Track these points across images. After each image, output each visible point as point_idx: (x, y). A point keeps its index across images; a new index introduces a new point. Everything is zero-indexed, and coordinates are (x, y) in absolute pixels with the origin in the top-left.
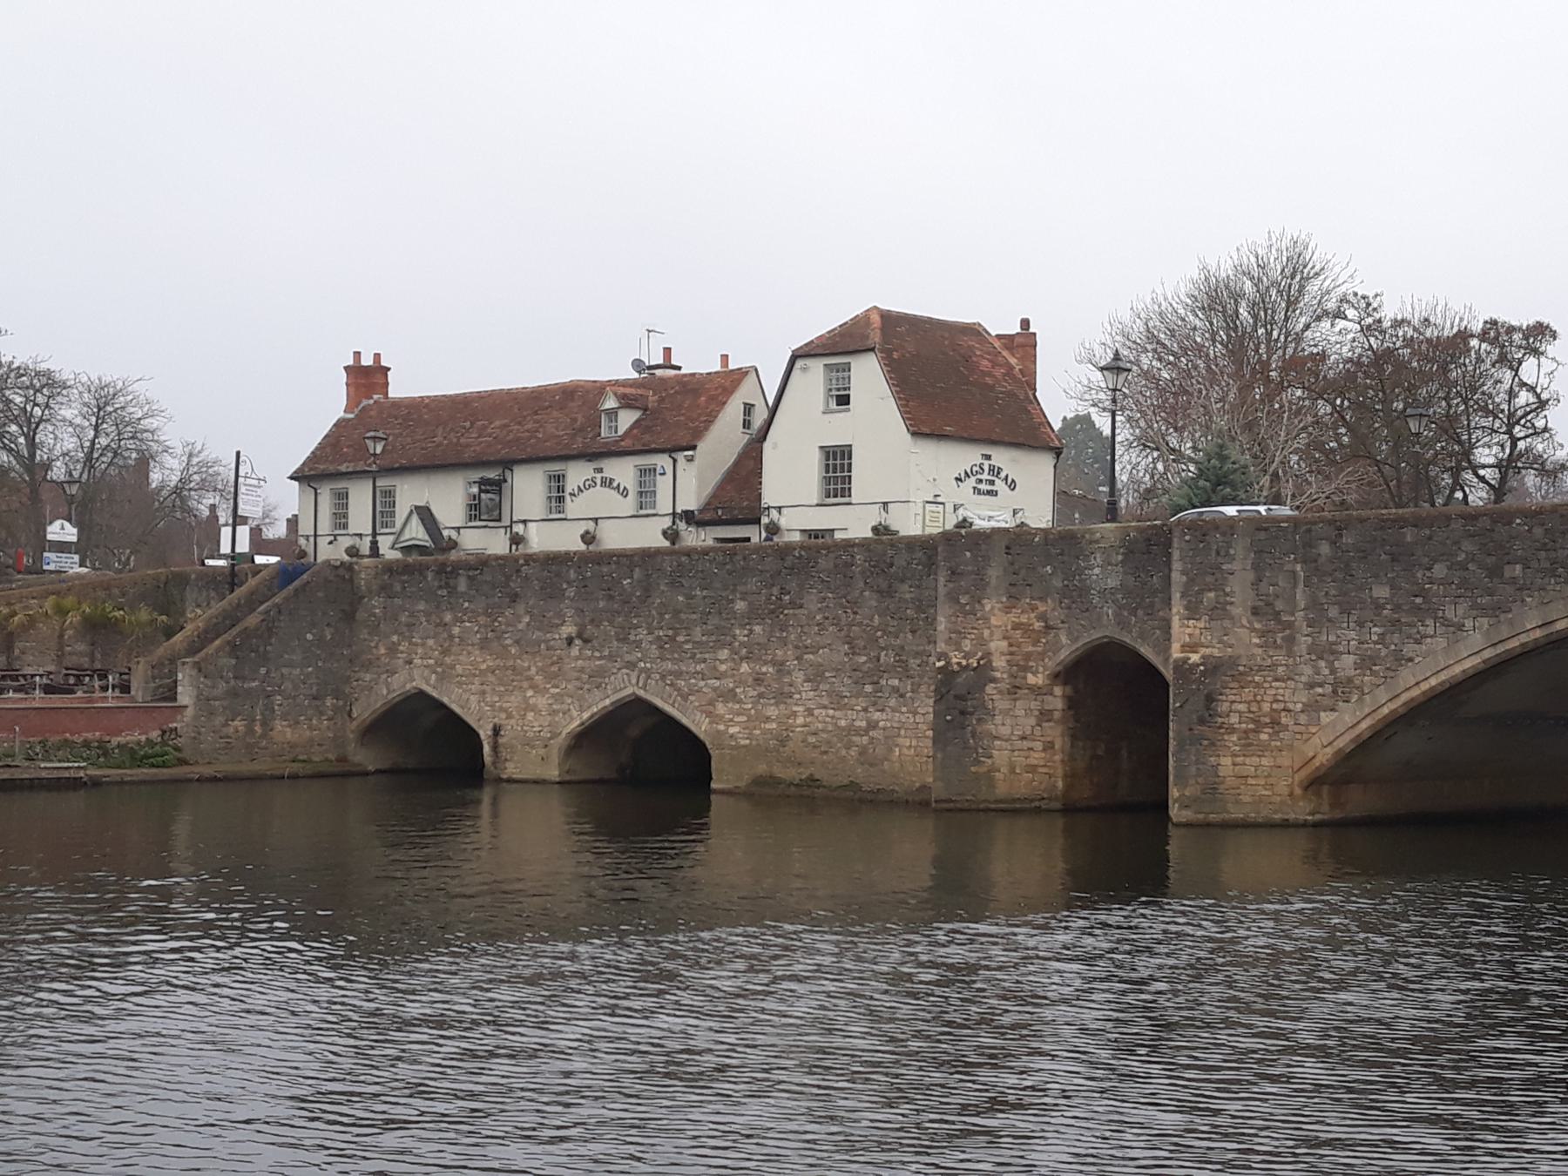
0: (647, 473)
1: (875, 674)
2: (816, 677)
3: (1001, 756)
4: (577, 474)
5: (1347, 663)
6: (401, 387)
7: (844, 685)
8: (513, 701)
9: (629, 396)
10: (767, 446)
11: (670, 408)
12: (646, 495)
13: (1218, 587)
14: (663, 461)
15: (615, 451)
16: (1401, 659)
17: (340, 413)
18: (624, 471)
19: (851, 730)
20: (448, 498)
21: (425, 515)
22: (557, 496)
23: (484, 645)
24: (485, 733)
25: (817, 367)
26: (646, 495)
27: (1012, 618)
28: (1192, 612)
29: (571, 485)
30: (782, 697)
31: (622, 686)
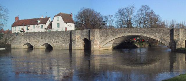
0: (42, 26)
1: (66, 41)
2: (61, 41)
3: (77, 47)
4: (36, 25)
5: (103, 40)
6: (20, 19)
7: (64, 42)
8: (35, 43)
9: (40, 19)
10: (52, 23)
11: (44, 21)
12: (42, 28)
13: (94, 34)
14: (43, 24)
15: (40, 24)
16: (107, 39)
17: (15, 21)
18: (40, 25)
19: (64, 45)
20: (25, 28)
21: (23, 29)
22: (34, 27)
23: (33, 39)
24: (33, 46)
25: (56, 18)
26: (42, 28)
27: (78, 36)
28: (92, 36)
29: (35, 26)
30: (58, 43)
31: (45, 42)
